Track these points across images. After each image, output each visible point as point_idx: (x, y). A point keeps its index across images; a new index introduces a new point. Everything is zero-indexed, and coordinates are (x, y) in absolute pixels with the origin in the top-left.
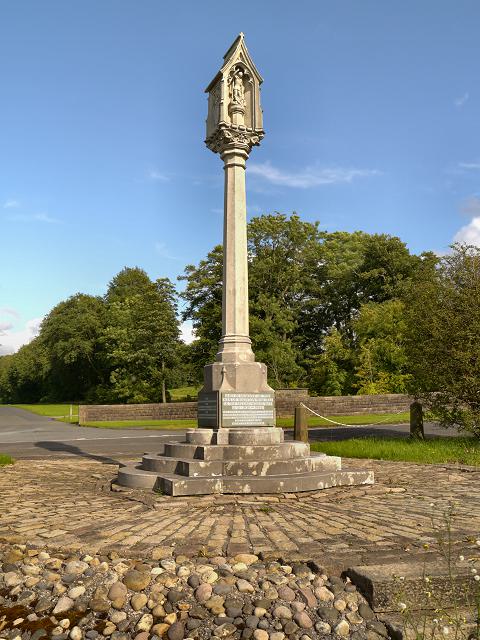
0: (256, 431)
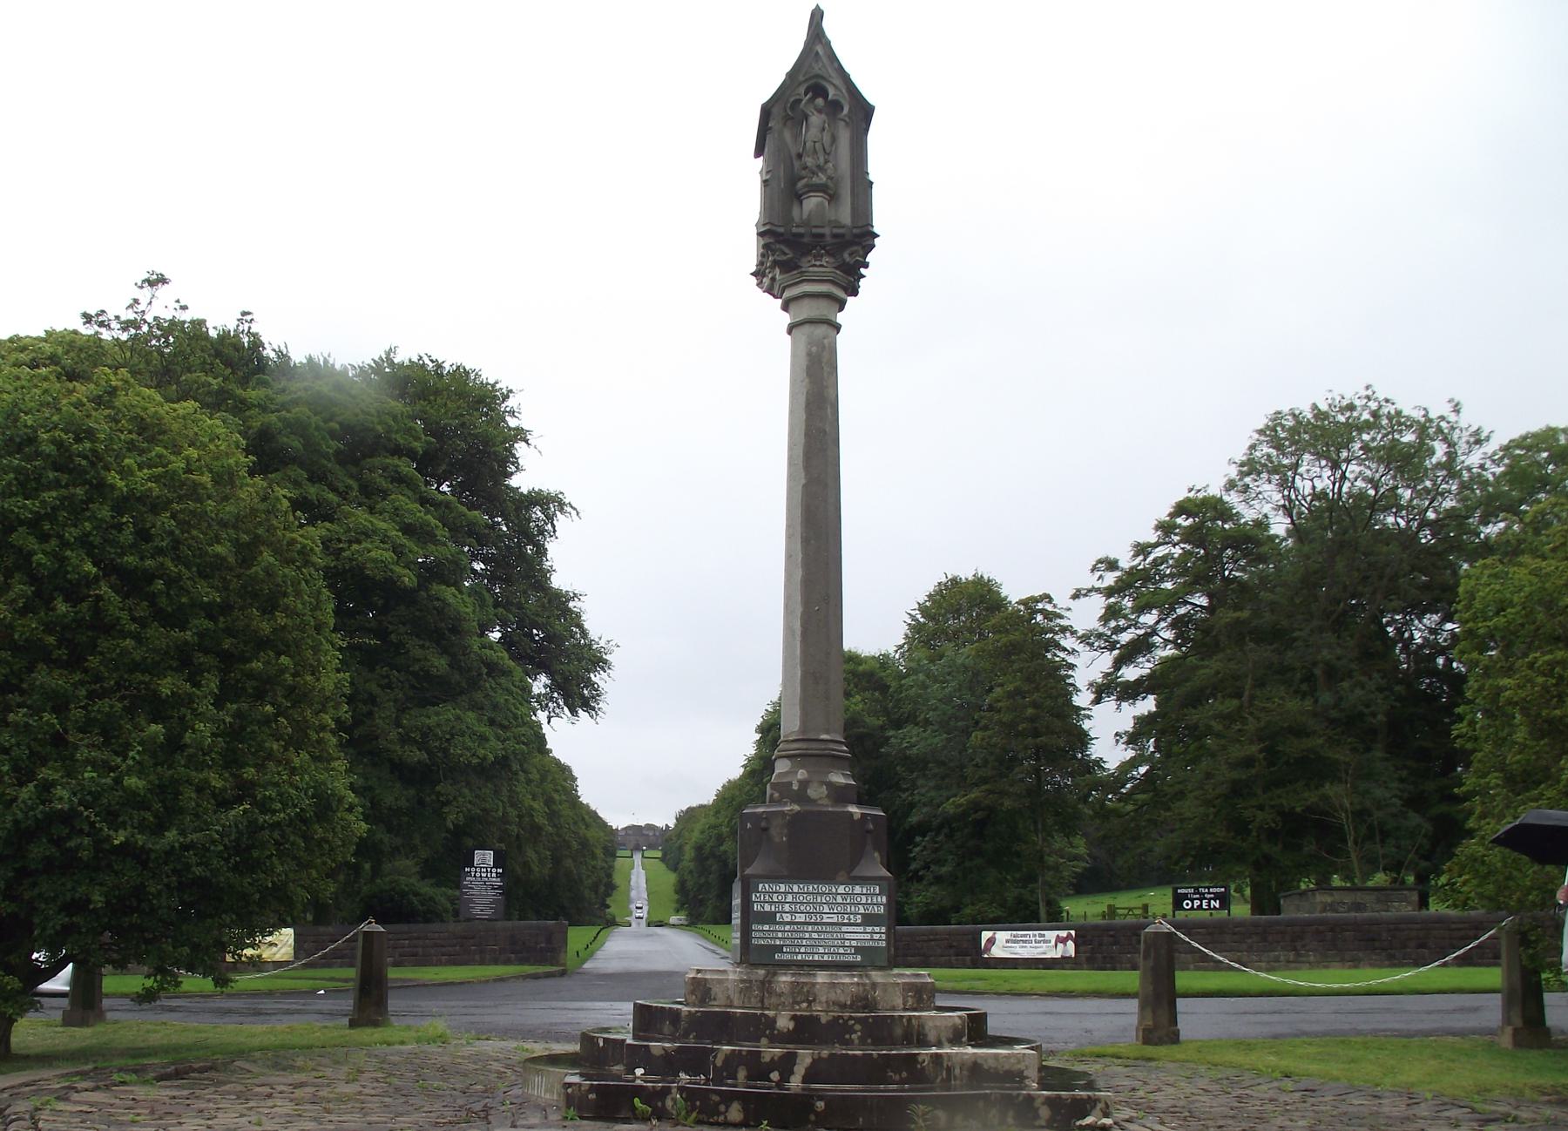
0: (821, 977)
